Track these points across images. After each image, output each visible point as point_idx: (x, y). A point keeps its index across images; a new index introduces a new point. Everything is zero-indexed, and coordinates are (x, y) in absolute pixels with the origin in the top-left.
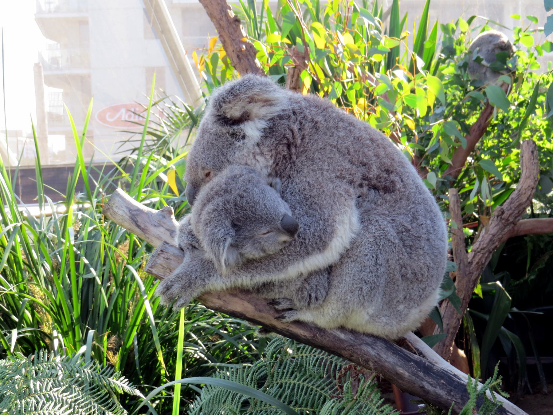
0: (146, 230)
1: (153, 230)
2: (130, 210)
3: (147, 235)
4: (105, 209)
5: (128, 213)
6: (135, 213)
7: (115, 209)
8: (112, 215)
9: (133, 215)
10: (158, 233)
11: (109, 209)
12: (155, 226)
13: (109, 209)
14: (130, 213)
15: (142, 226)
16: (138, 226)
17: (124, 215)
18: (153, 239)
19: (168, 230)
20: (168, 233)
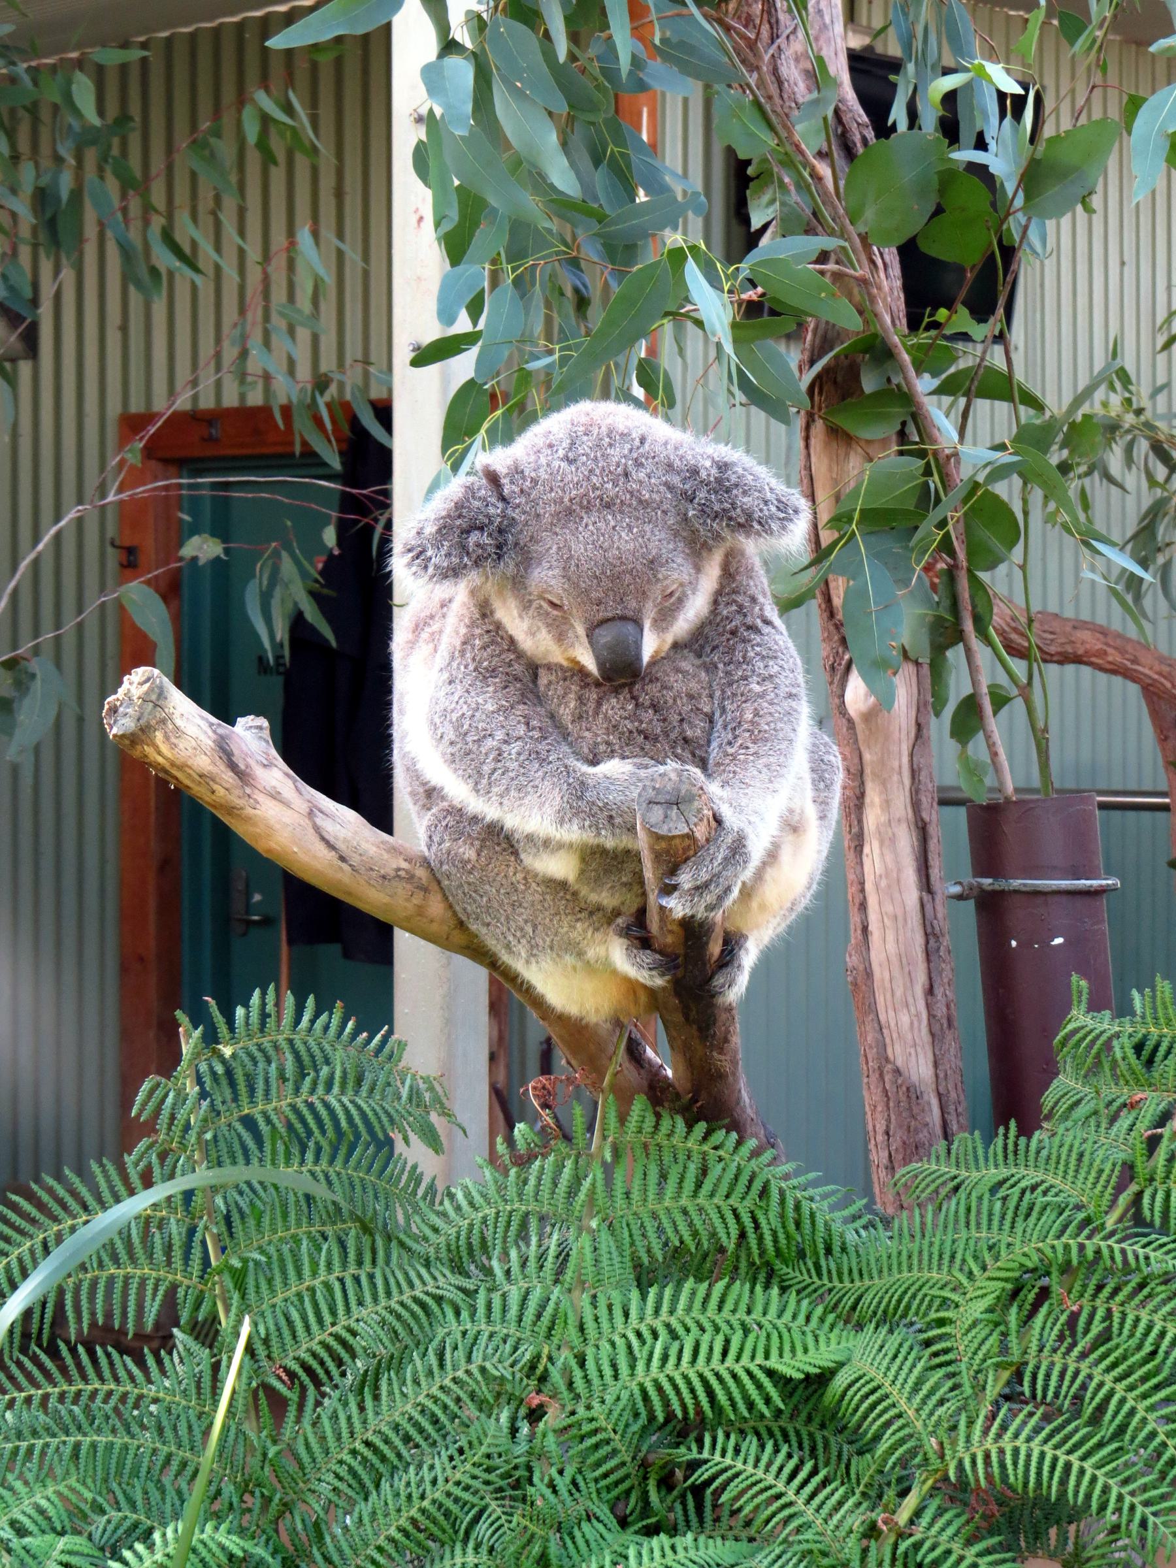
0: (249, 775)
1: (260, 773)
2: (211, 725)
3: (248, 790)
4: (153, 722)
5: (210, 733)
6: (220, 731)
7: (179, 722)
8: (167, 738)
9: (222, 737)
10: (274, 783)
11: (163, 721)
12: (265, 766)
13: (163, 721)
14: (215, 732)
15: (242, 767)
16: (233, 766)
17: (202, 737)
18: (261, 797)
19: (287, 775)
20: (290, 783)
